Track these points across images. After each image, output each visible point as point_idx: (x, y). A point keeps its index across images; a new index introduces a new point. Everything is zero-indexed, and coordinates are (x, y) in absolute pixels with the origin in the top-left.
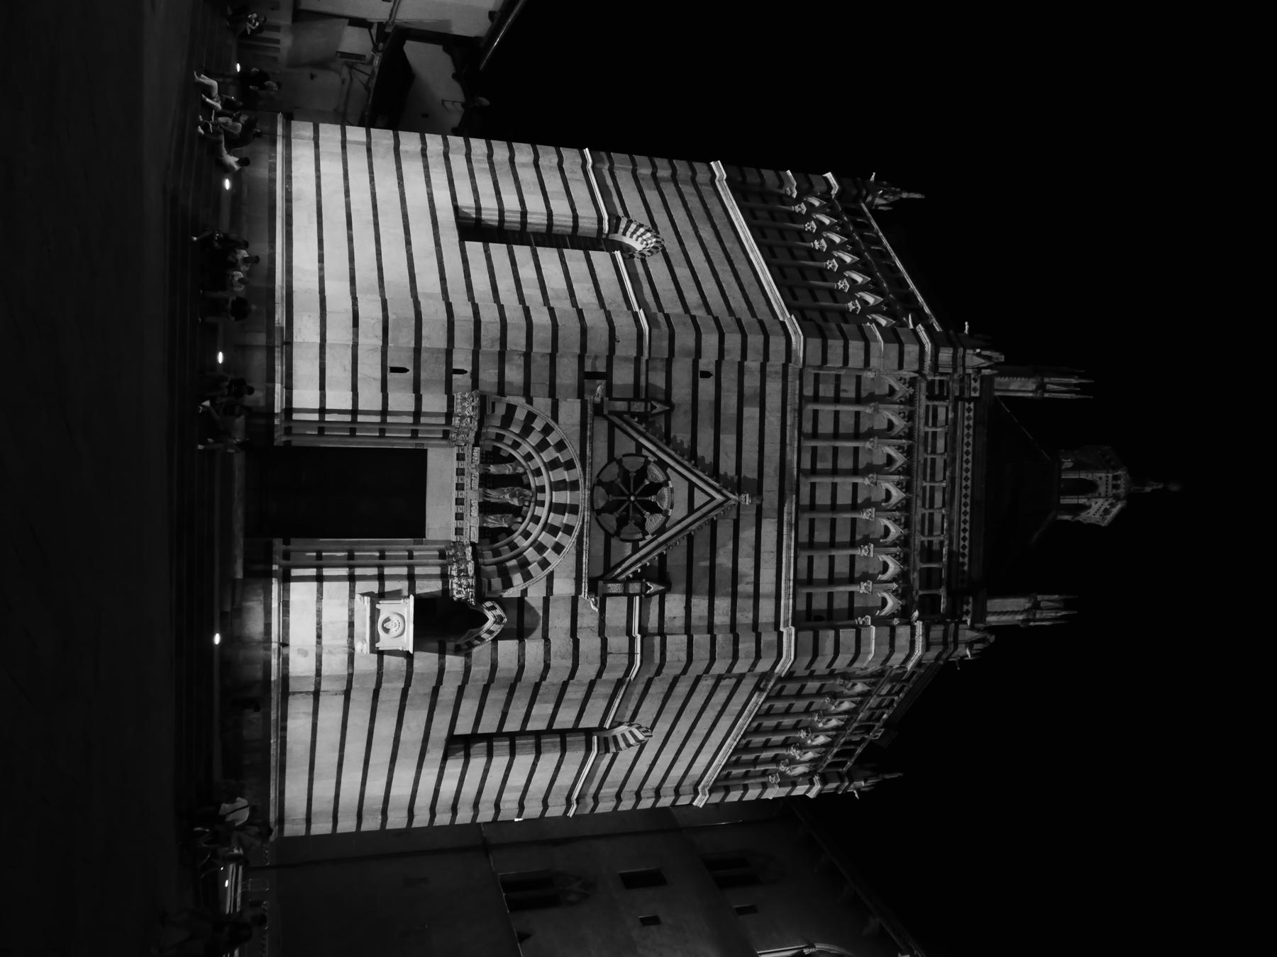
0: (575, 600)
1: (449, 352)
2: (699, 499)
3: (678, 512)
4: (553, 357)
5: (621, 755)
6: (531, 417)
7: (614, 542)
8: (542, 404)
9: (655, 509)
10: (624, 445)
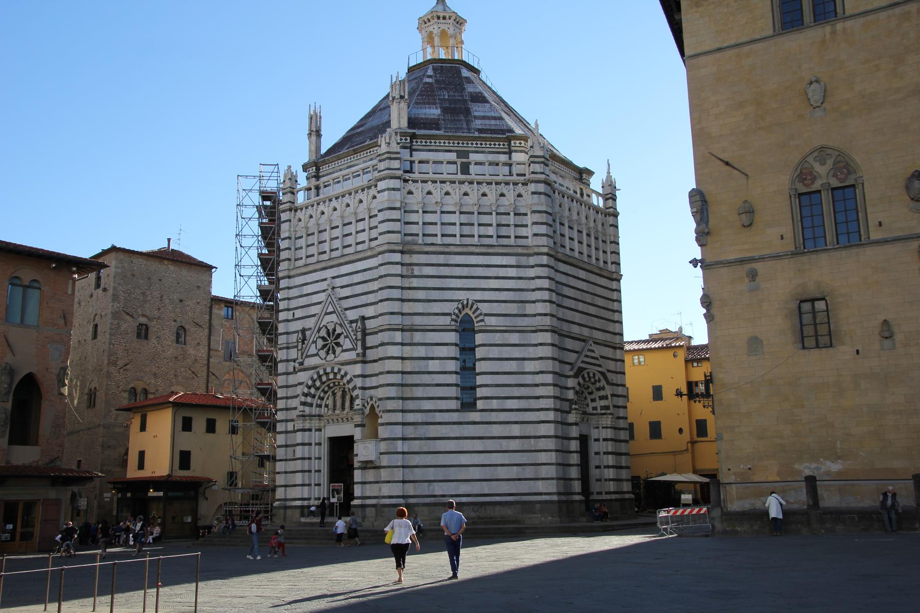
0: (364, 362)
1: (287, 432)
2: (330, 309)
3: (333, 318)
4: (287, 387)
5: (484, 312)
6: (305, 395)
7: (344, 348)
8: (299, 390)
9: (334, 330)
10: (313, 350)
